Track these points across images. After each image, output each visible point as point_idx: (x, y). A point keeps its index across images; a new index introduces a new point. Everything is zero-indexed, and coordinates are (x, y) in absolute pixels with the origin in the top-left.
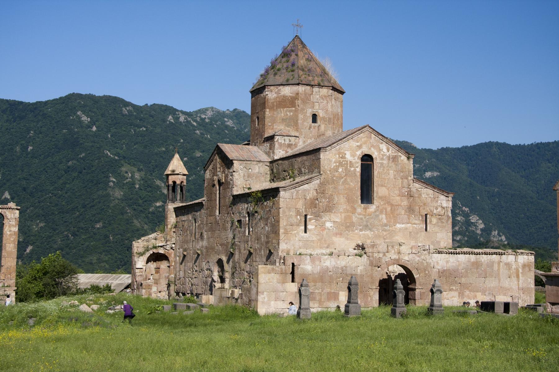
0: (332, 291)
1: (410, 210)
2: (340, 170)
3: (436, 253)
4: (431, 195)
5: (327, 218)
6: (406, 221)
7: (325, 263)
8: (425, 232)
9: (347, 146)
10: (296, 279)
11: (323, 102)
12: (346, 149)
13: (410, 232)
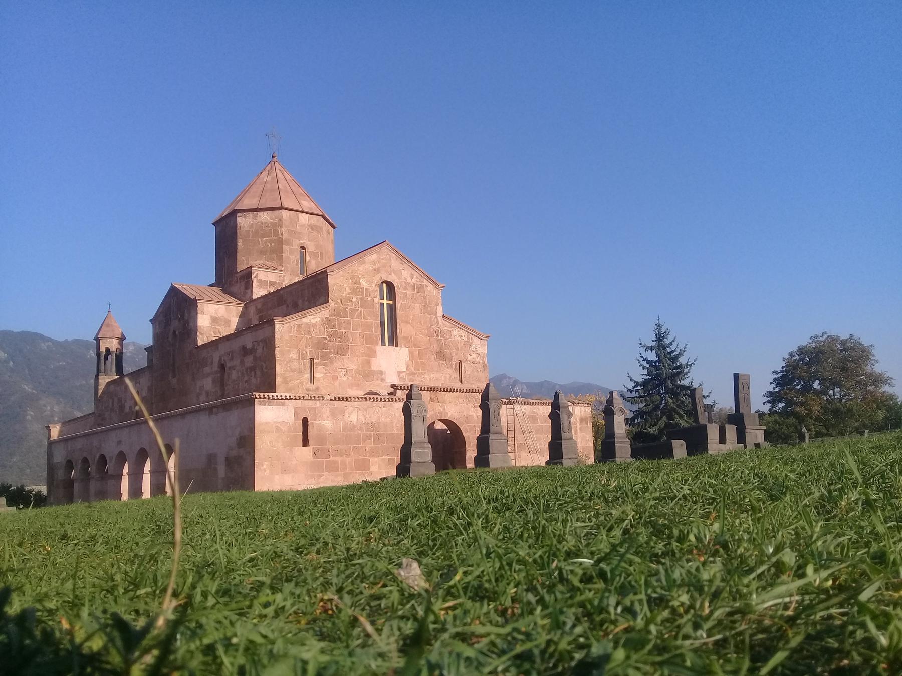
0: (361, 457)
1: (441, 355)
2: (354, 300)
5: (340, 364)
7: (349, 417)
9: (361, 268)
10: (311, 442)
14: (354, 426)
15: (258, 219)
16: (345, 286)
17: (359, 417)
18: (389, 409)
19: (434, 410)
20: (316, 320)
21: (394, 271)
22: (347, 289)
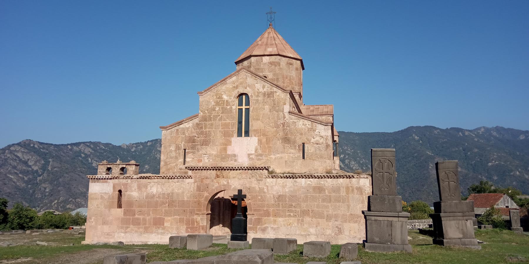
0: (158, 216)
1: (286, 140)
2: (217, 109)
3: (270, 178)
4: (308, 124)
6: (281, 151)
7: (151, 189)
8: (301, 161)
9: (223, 88)
11: (271, 67)
12: (224, 90)
13: (286, 161)
14: (154, 196)
15: (243, 65)
16: (211, 101)
17: (158, 189)
18: (181, 184)
19: (218, 183)
20: (189, 125)
21: (249, 86)
22: (213, 102)
